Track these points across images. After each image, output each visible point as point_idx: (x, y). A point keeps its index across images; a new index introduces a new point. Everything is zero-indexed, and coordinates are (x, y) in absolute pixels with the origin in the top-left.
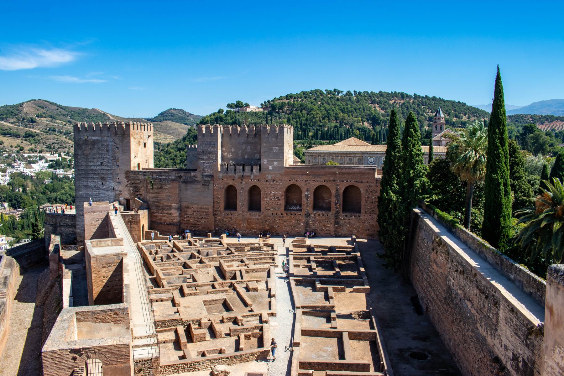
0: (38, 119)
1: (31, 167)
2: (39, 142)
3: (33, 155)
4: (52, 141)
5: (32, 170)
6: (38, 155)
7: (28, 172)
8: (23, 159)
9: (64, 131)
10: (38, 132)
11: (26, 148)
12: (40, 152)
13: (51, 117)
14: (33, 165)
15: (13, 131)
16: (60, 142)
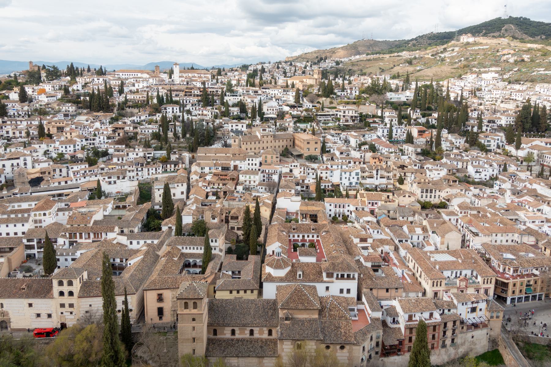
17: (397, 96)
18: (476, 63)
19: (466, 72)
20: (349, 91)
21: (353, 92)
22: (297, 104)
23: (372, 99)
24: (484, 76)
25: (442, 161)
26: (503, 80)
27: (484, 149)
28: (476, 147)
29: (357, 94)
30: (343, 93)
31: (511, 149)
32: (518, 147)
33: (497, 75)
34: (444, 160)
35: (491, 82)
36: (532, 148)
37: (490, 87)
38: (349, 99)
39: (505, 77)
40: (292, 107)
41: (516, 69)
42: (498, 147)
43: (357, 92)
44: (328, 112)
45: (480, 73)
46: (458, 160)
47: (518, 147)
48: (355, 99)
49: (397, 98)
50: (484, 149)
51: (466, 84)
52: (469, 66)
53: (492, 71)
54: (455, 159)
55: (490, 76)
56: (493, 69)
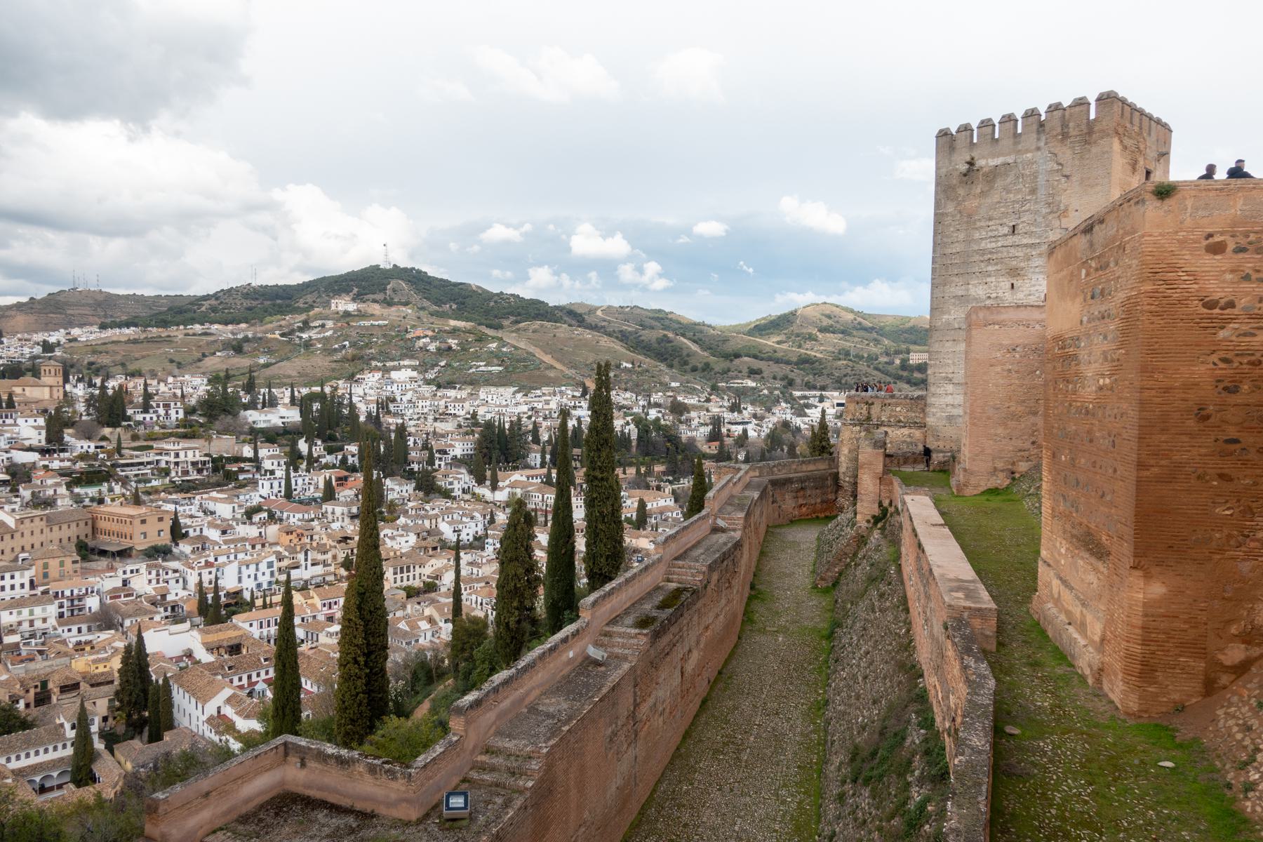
0: (820, 335)
1: (805, 415)
2: (821, 374)
3: (807, 393)
4: (844, 372)
5: (806, 419)
6: (818, 393)
7: (798, 421)
8: (791, 400)
9: (866, 355)
10: (819, 355)
11: (798, 381)
12: (823, 388)
13: (842, 332)
14: (806, 410)
15: (779, 355)
16: (858, 372)
17: (263, 417)
18: (373, 351)
19: (361, 368)
20: (161, 411)
21: (172, 412)
22: (54, 444)
23: (217, 425)
24: (394, 375)
25: (398, 522)
26: (428, 382)
27: (447, 494)
28: (437, 495)
29: (181, 415)
30: (148, 416)
31: (484, 491)
32: (494, 487)
33: (415, 374)
34: (402, 520)
35: (408, 387)
36: (512, 486)
37: (409, 395)
38: (164, 427)
39: (431, 375)
40: (43, 452)
41: (442, 364)
42: (464, 491)
43: (181, 413)
44: (132, 457)
45: (386, 370)
46: (423, 518)
47: (494, 487)
48: (178, 426)
49: (264, 421)
50: (447, 494)
51: (366, 391)
52: (362, 357)
53: (405, 367)
54: (417, 516)
55: (404, 375)
56: (406, 362)
